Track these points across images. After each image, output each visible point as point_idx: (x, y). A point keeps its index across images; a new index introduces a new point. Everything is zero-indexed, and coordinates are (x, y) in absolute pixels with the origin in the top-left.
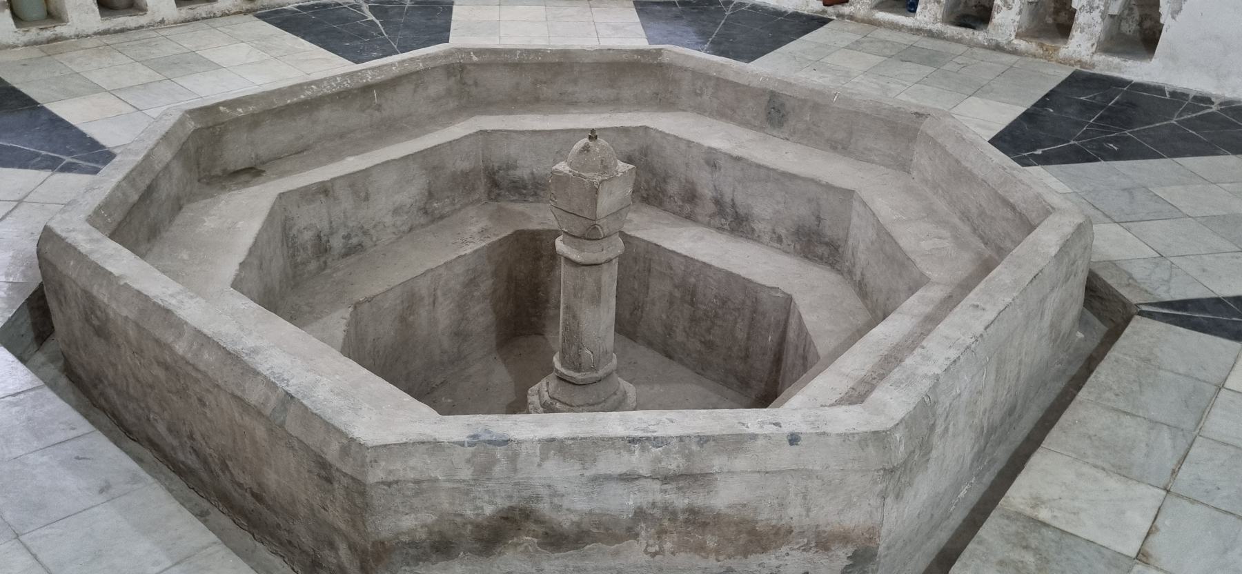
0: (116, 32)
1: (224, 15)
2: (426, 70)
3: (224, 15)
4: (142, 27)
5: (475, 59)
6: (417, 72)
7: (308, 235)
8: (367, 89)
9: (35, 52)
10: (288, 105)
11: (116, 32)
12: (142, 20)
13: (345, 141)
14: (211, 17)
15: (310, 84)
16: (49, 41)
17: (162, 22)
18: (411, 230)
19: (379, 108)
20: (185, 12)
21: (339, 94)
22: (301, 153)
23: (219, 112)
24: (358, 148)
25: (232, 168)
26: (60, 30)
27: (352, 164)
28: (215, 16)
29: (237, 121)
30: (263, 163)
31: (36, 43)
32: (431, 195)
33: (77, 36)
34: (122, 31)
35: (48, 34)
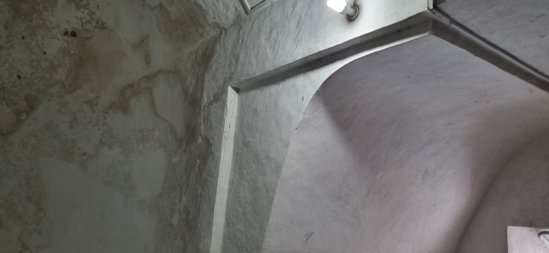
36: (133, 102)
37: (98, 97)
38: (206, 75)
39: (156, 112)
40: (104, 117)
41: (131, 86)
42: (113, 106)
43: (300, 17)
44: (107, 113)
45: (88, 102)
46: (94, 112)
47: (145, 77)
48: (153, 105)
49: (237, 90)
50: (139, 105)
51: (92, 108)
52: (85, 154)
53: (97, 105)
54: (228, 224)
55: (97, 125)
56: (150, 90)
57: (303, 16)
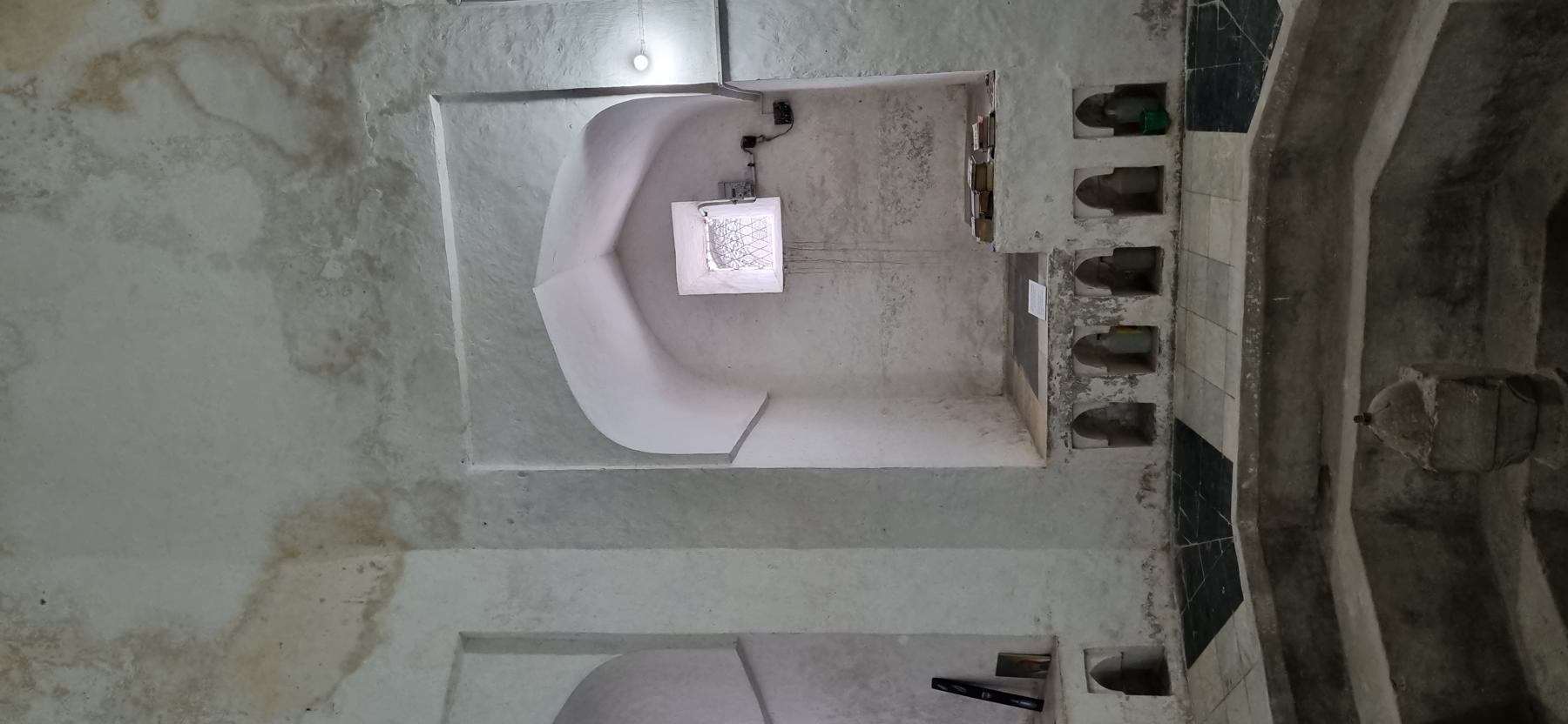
0: (1176, 284)
1: (1180, 160)
2: (1268, 214)
3: (1180, 160)
4: (1176, 256)
5: (1272, 136)
6: (1268, 229)
7: (1418, 483)
8: (1270, 311)
9: (1177, 366)
10: (1261, 419)
11: (1176, 284)
12: (1169, 254)
13: (1326, 349)
14: (1180, 176)
15: (1244, 380)
16: (1173, 348)
17: (1175, 233)
18: (1479, 329)
19: (1299, 295)
20: (1169, 206)
21: (1264, 350)
22: (1322, 409)
23: (1246, 491)
24: (1339, 341)
25: (1312, 493)
26: (1164, 335)
27: (1351, 387)
28: (1180, 172)
29: (1263, 479)
30: (1320, 455)
31: (1172, 360)
32: (1439, 293)
33: (1173, 322)
34: (1176, 277)
35: (1165, 348)
36: (130, 88)
37: (33, 80)
38: (354, 66)
39: (199, 108)
40: (64, 119)
41: (115, 57)
42: (77, 96)
43: (562, 40)
44: (69, 111)
45: (10, 92)
46: (34, 110)
47: (145, 41)
48: (186, 94)
49: (437, 98)
50: (151, 98)
51: (25, 103)
52: (43, 193)
53: (34, 96)
54: (464, 261)
55: (52, 136)
56: (171, 69)
57: (568, 41)
